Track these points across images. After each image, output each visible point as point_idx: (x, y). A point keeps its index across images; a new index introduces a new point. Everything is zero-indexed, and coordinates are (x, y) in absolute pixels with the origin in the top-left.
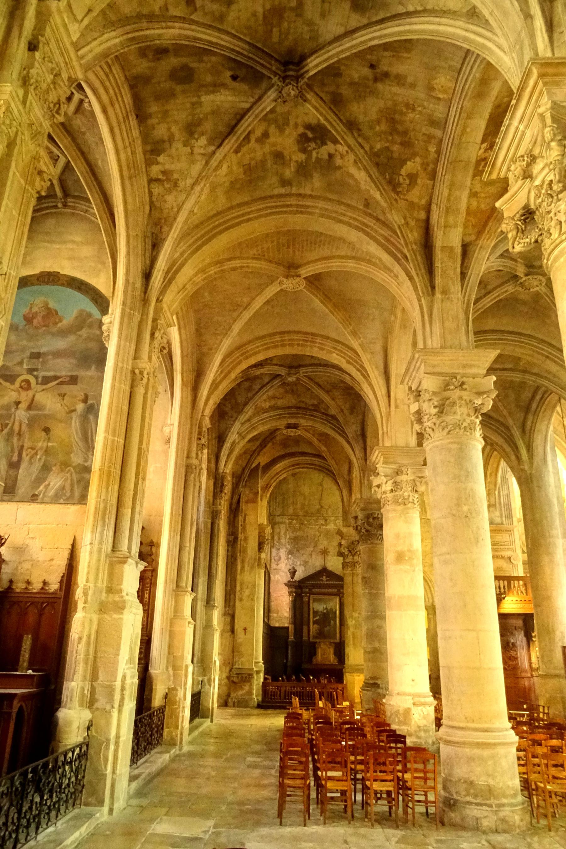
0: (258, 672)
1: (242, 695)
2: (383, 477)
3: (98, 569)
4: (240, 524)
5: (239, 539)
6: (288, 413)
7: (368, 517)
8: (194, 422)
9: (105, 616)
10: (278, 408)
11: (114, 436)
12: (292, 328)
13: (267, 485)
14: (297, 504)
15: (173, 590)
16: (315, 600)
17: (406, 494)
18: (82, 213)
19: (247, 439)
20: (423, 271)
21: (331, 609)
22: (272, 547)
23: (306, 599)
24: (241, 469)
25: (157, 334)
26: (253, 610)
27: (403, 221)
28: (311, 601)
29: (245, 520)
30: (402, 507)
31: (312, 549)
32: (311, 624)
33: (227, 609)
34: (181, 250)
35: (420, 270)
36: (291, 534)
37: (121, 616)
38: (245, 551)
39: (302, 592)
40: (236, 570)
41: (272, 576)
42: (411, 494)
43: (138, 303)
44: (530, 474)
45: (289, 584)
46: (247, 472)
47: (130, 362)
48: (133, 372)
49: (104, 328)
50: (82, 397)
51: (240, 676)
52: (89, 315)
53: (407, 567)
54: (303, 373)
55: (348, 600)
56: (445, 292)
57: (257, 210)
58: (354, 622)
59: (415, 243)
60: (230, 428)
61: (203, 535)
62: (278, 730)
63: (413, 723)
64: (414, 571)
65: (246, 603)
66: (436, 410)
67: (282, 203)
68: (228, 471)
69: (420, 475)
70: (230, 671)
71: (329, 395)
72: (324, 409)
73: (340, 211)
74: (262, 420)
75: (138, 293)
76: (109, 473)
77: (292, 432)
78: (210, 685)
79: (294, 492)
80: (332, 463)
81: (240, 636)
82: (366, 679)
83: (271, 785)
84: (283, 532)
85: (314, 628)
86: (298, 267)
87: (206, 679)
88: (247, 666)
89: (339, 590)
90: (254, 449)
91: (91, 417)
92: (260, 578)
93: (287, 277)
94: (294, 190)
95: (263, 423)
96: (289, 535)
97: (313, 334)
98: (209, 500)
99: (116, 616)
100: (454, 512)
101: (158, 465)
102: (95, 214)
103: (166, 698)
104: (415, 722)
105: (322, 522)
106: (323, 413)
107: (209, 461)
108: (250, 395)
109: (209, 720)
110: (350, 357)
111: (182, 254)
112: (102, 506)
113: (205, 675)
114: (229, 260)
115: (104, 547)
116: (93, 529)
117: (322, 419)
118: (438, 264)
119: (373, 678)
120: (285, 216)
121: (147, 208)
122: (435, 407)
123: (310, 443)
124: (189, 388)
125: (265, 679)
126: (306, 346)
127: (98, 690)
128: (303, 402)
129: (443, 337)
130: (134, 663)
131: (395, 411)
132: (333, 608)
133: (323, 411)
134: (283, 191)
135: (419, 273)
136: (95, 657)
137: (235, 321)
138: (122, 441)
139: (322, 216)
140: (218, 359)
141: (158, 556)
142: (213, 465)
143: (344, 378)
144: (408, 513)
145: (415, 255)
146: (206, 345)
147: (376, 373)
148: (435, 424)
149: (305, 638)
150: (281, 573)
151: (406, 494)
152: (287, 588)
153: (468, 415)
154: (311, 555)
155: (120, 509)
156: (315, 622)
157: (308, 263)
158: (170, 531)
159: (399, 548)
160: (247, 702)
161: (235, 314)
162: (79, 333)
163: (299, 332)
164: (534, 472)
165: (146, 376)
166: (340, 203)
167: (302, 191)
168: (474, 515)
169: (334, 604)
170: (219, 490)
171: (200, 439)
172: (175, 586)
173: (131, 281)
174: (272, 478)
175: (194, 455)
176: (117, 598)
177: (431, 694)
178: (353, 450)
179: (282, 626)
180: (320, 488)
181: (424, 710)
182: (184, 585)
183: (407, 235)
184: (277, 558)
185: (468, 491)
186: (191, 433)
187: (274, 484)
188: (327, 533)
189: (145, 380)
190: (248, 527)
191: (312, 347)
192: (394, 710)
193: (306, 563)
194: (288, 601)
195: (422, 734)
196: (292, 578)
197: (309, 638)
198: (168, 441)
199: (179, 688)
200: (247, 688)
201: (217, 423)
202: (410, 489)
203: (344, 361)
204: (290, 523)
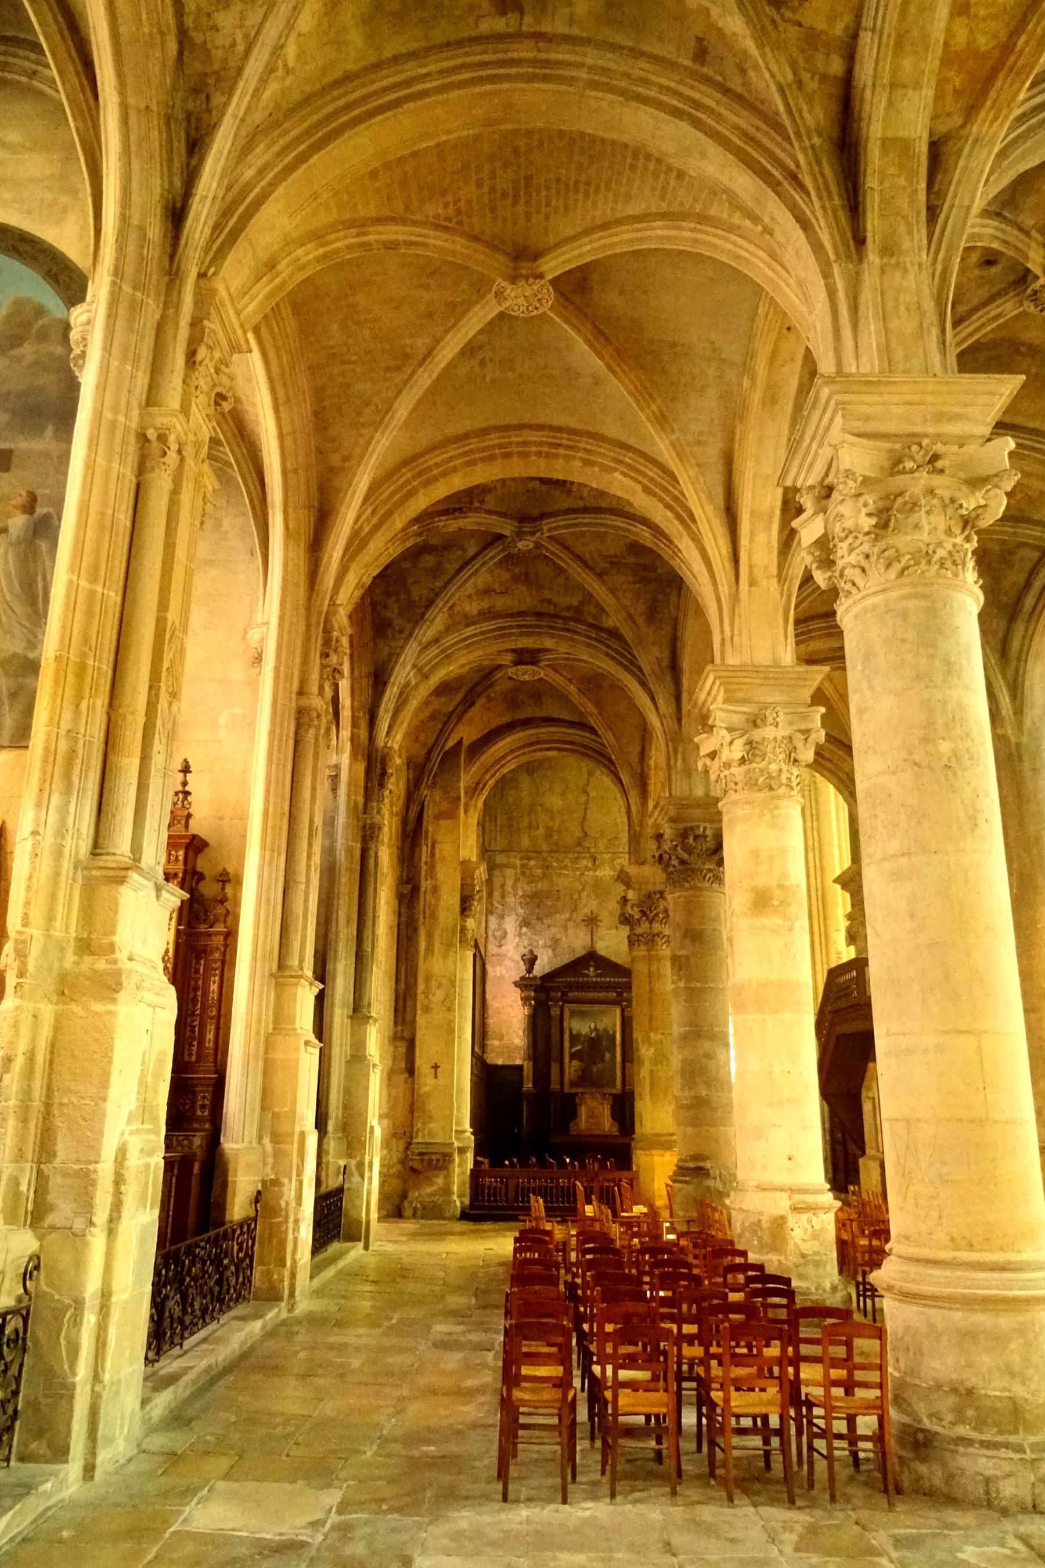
0: (462, 1151)
1: (432, 1195)
2: (725, 732)
3: (53, 896)
4: (424, 859)
5: (422, 889)
6: (519, 627)
7: (684, 834)
8: (314, 620)
9: (73, 1007)
10: (498, 616)
11: (93, 578)
12: (527, 418)
13: (478, 784)
15: (271, 975)
16: (573, 1013)
17: (773, 767)
18: (24, 79)
19: (435, 680)
20: (837, 201)
21: (605, 1030)
22: (489, 912)
23: (555, 1012)
24: (423, 752)
25: (202, 353)
26: (451, 1030)
27: (790, 77)
28: (566, 1016)
29: (433, 855)
30: (766, 794)
31: (567, 916)
32: (567, 1059)
33: (399, 1028)
34: (260, 163)
35: (830, 198)
37: (112, 1007)
38: (433, 915)
39: (549, 999)
40: (417, 951)
41: (489, 968)
42: (785, 767)
43: (155, 276)
44: (1018, 745)
45: (523, 984)
46: (436, 758)
47: (135, 413)
48: (143, 438)
49: (74, 335)
50: (21, 499)
51: (426, 1157)
52: (40, 311)
53: (777, 921)
54: (549, 530)
55: (639, 1011)
56: (888, 250)
57: (440, 72)
59: (820, 135)
60: (399, 655)
61: (343, 872)
62: (501, 1264)
63: (791, 1246)
64: (791, 929)
65: (438, 1015)
66: (873, 521)
67: (500, 56)
68: (396, 747)
69: (803, 727)
70: (407, 1148)
71: (603, 583)
72: (595, 617)
73: (636, 73)
74: (466, 639)
75: (154, 253)
76: (81, 670)
77: (526, 674)
78: (362, 1176)
79: (533, 804)
80: (608, 737)
81: (426, 1081)
82: (680, 1160)
83: (480, 1390)
84: (509, 883)
85: (572, 1068)
86: (537, 256)
87: (353, 1162)
89: (620, 994)
90: (451, 708)
91: (43, 545)
92: (464, 965)
93: (513, 280)
94: (528, 23)
95: (467, 647)
97: (571, 431)
98: (356, 803)
99: (98, 1007)
100: (916, 757)
101: (238, 711)
102: (54, 81)
103: (257, 1201)
104: (796, 1244)
105: (586, 863)
106: (592, 626)
107: (355, 724)
108: (439, 584)
109: (361, 1245)
110: (652, 480)
111: (261, 172)
112: (63, 746)
113: (350, 1156)
114: (378, 221)
115: (69, 844)
116: (40, 798)
117: (589, 637)
118: (871, 182)
119: (695, 1157)
120: (506, 86)
121: (173, 47)
122: (869, 515)
123: (564, 699)
124: (302, 545)
125: (476, 1163)
126: (555, 456)
127: (56, 1181)
128: (550, 601)
129: (886, 351)
130: (154, 1119)
131: (750, 593)
133: (591, 621)
134: (500, 25)
135: (827, 205)
136: (48, 1106)
137: (399, 392)
138: (114, 597)
139: (594, 85)
140: (362, 483)
141: (237, 903)
142: (363, 733)
143: (637, 534)
144: (777, 807)
145: (819, 163)
146: (335, 451)
147: (709, 509)
148: (867, 556)
149: (555, 1086)
150: (507, 963)
151: (773, 767)
152: (518, 990)
153: (949, 532)
154: (566, 928)
155: (112, 758)
156: (573, 1056)
157: (558, 245)
158: (263, 847)
159: (761, 881)
161: (398, 378)
162: (15, 352)
163: (541, 427)
164: (1025, 740)
165: (174, 447)
166: (637, 53)
167: (546, 27)
168: (967, 763)
169: (611, 1020)
170: (376, 781)
171: (327, 655)
172: (275, 967)
173: (135, 221)
175: (315, 689)
176: (101, 965)
177: (828, 1186)
178: (653, 699)
179: (509, 1063)
180: (584, 799)
181: (814, 1219)
182: (296, 963)
183: (800, 111)
184: (498, 934)
185: (949, 707)
186: (307, 638)
187: (491, 783)
188: (598, 883)
189: (172, 456)
191: (567, 458)
192: (752, 1220)
193: (555, 943)
194: (520, 1016)
195: (811, 1270)
196: (530, 970)
197: (562, 1085)
198: (258, 659)
199: (285, 1181)
200: (440, 1181)
201: (371, 645)
202: (782, 757)
203: (639, 488)
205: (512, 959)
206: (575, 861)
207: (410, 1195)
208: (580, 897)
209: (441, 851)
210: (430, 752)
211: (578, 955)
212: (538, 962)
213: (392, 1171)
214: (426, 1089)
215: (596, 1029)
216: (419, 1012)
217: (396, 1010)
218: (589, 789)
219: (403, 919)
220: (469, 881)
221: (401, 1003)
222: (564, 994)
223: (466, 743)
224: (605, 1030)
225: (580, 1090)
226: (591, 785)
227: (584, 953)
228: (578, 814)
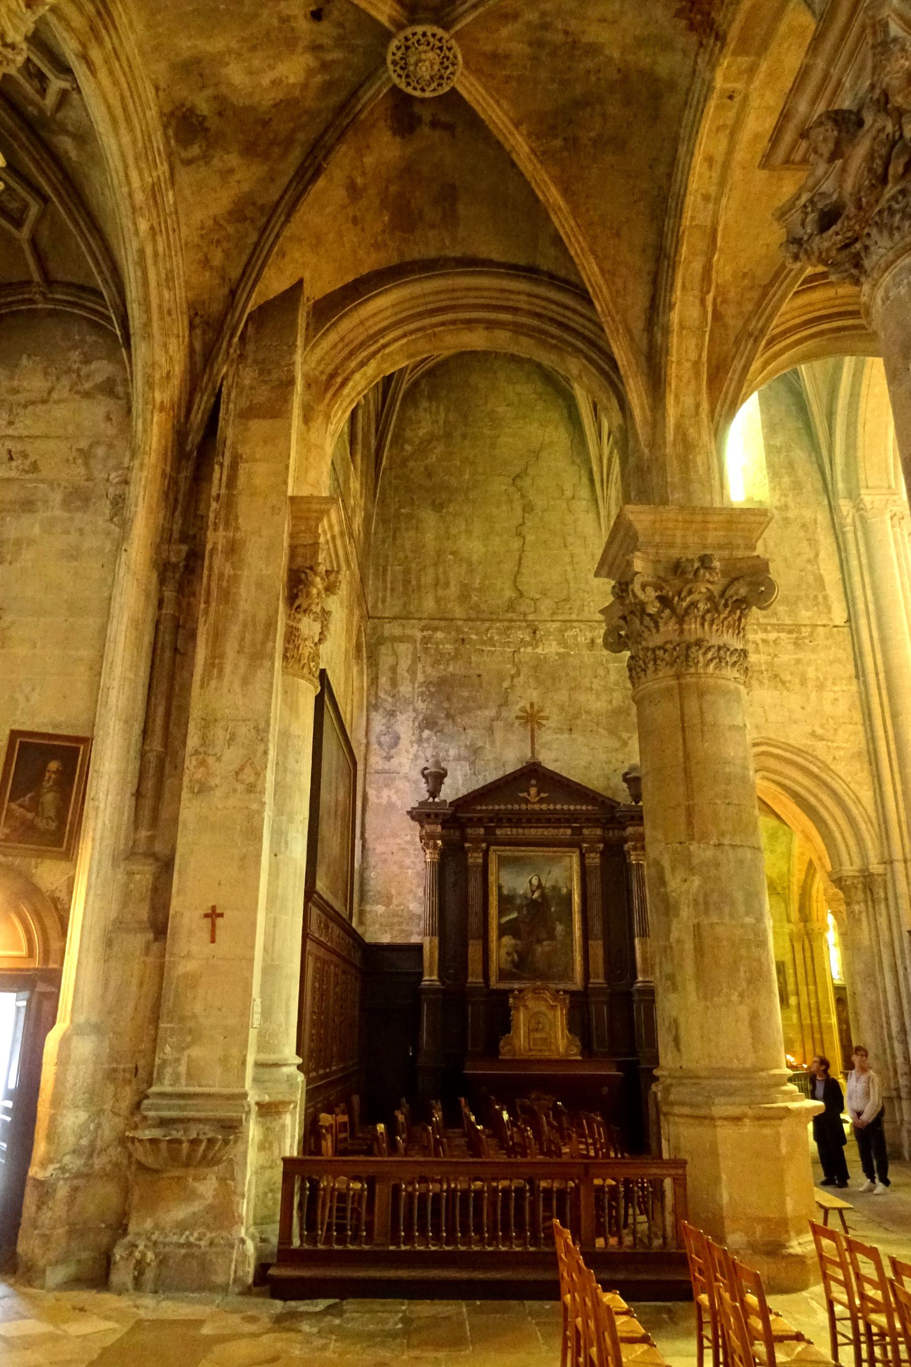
0: (269, 1110)
1: (182, 1226)
4: (214, 492)
13: (332, 376)
14: (447, 584)
16: (503, 862)
22: (373, 707)
23: (474, 859)
28: (493, 867)
29: (232, 482)
31: (491, 712)
32: (494, 934)
36: (429, 670)
38: (227, 596)
39: (464, 838)
45: (420, 815)
58: (696, 881)
70: (138, 1106)
79: (439, 553)
84: (404, 664)
88: (214, 1083)
89: (577, 831)
90: (276, 197)
92: (292, 705)
96: (426, 671)
105: (523, 635)
132: (561, 884)
149: (474, 979)
150: (400, 784)
152: (416, 825)
154: (491, 730)
156: (503, 931)
160: (205, 1265)
174: (351, 354)
179: (400, 940)
180: (516, 544)
184: (385, 739)
188: (538, 665)
190: (243, 504)
194: (420, 866)
196: (434, 793)
204: (426, 641)
205: (406, 777)
206: (505, 631)
207: (132, 1228)
208: (512, 687)
209: (249, 475)
210: (233, 293)
211: (510, 770)
212: (447, 780)
213: (98, 1163)
214: (190, 966)
215: (540, 886)
216: (185, 795)
217: (138, 795)
218: (525, 530)
219: (169, 610)
220: (308, 539)
221: (150, 784)
222: (489, 831)
223: (313, 291)
224: (554, 888)
225: (516, 986)
226: (529, 524)
227: (519, 767)
228: (508, 567)
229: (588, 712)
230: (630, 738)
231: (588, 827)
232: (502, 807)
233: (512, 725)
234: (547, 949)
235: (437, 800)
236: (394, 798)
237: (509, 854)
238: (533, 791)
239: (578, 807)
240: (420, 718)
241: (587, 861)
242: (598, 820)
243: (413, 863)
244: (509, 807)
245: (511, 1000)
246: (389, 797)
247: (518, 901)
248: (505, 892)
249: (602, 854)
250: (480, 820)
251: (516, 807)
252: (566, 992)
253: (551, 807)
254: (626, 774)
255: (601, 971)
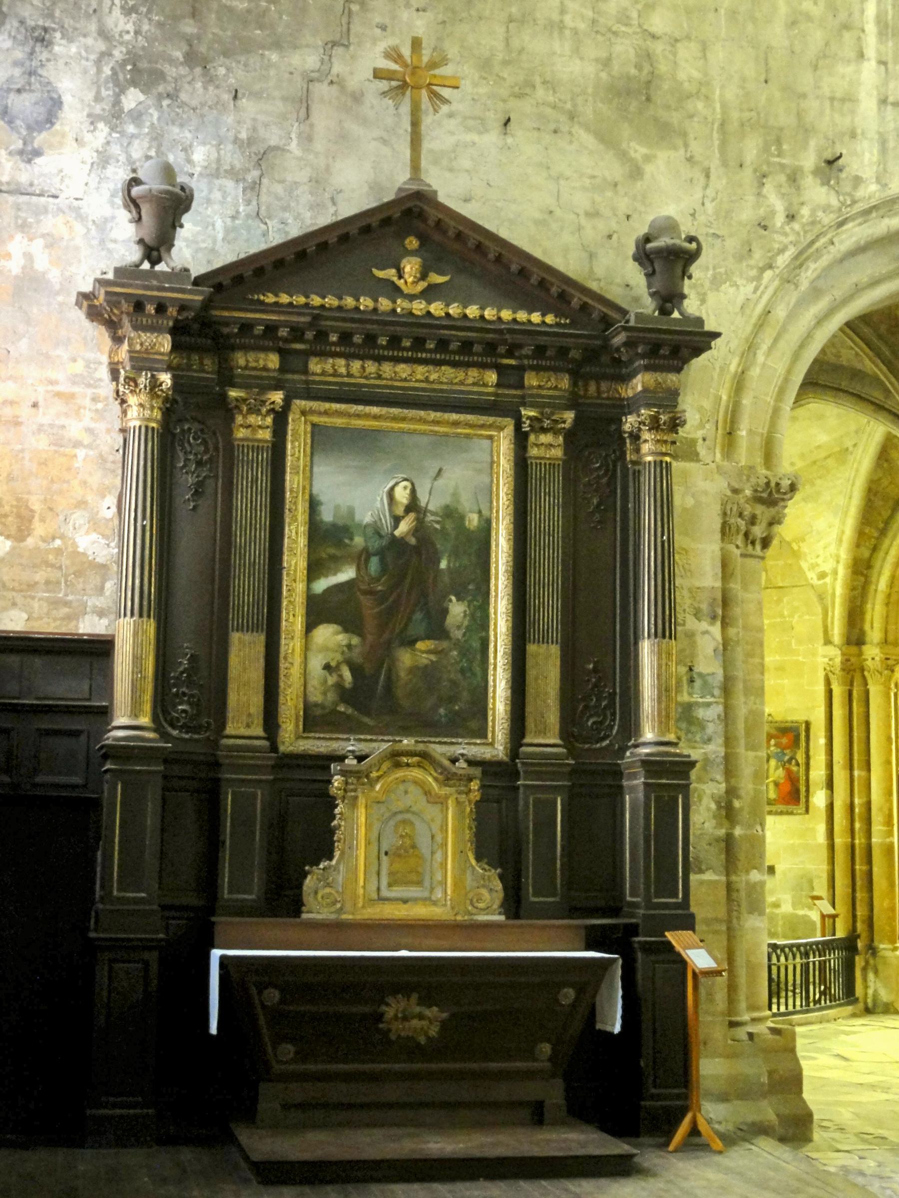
21: (451, 513)
31: (310, 60)
39: (227, 378)
132: (466, 503)
152: (99, 334)
211: (347, 210)
215: (413, 506)
224: (451, 513)
225: (351, 745)
229: (550, 84)
230: (648, 159)
231: (537, 369)
232: (331, 301)
233: (357, 98)
234: (425, 659)
235: (161, 267)
236: (42, 263)
237: (339, 422)
238: (411, 266)
239: (522, 316)
240: (118, 54)
241: (533, 452)
242: (563, 352)
243: (90, 431)
244: (349, 302)
245: (337, 781)
246: (28, 257)
247: (359, 541)
248: (327, 516)
249: (570, 436)
250: (271, 329)
251: (366, 303)
252: (471, 763)
253: (454, 310)
254: (647, 239)
255: (553, 718)
